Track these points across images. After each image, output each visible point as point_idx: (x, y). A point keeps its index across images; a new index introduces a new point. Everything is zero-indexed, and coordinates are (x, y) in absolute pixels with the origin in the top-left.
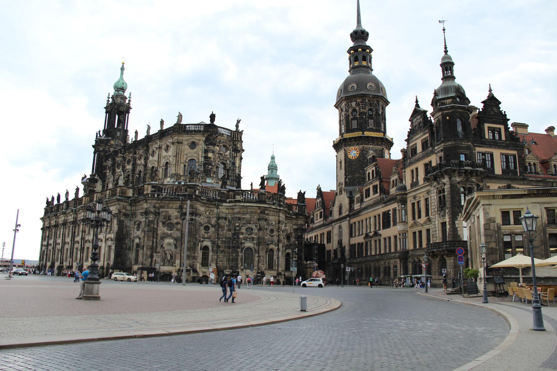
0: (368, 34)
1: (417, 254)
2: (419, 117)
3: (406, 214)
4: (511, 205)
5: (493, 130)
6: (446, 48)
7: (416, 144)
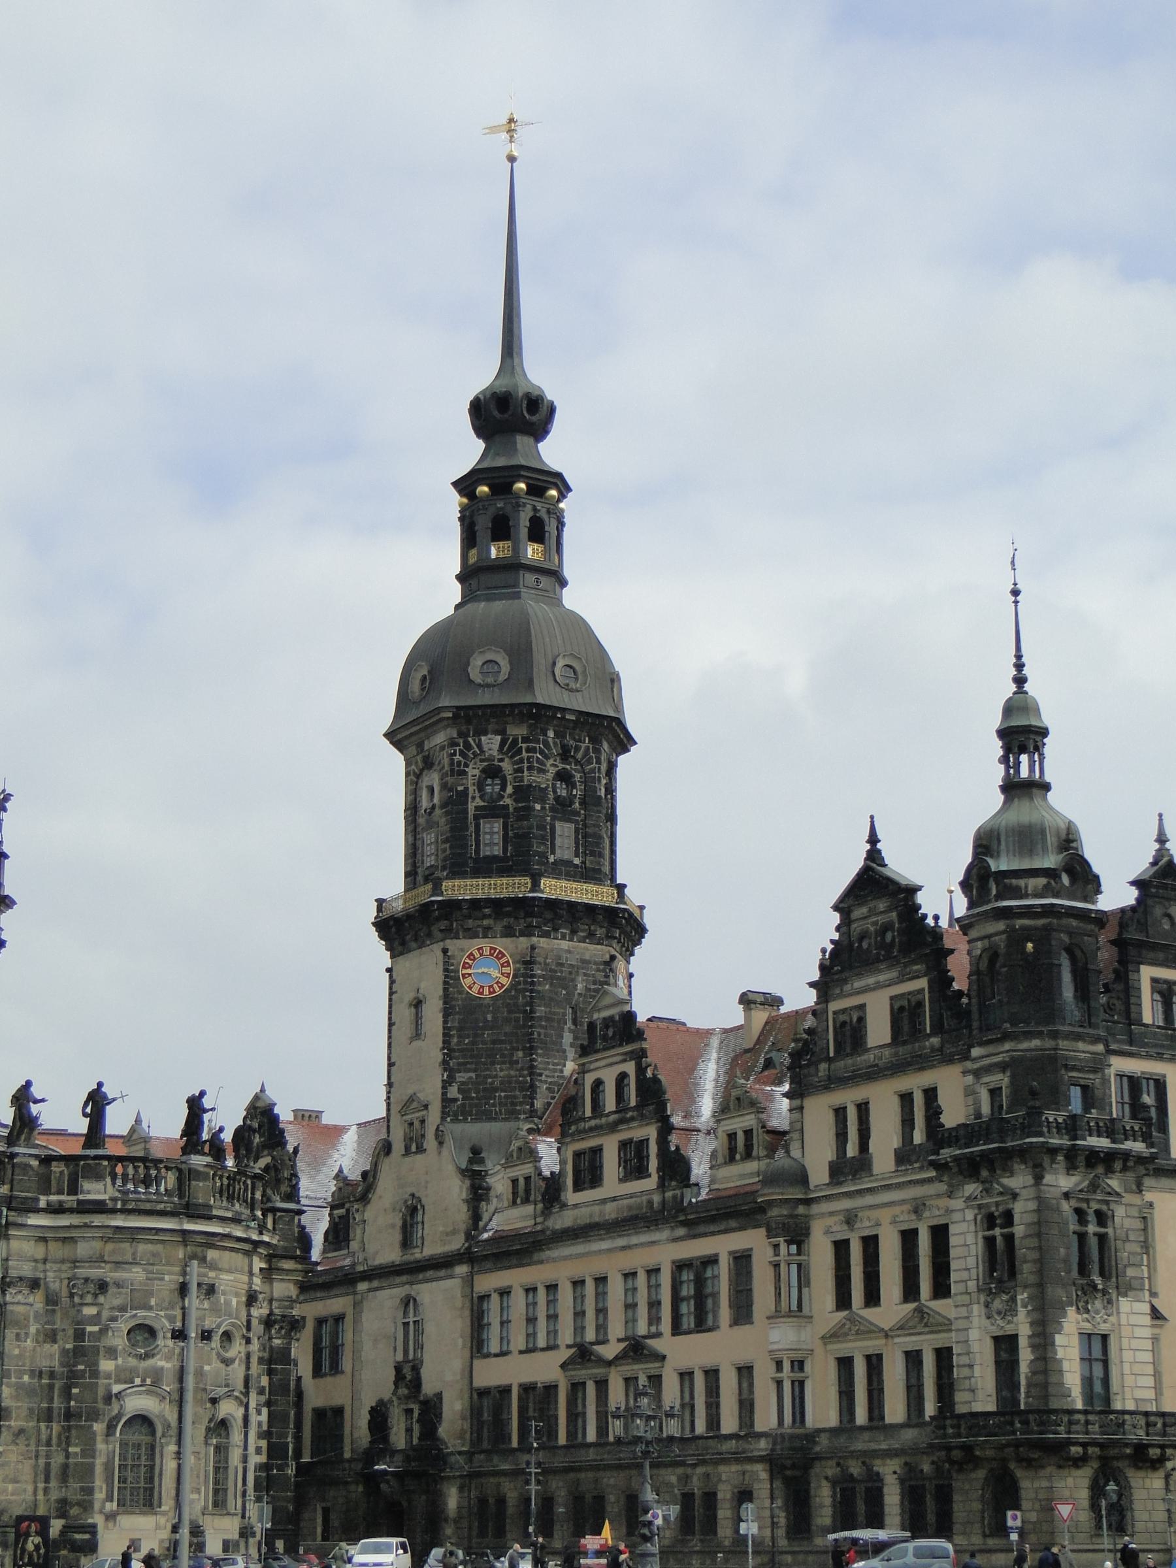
0: (552, 410)
1: (859, 1446)
2: (882, 906)
3: (804, 1279)
6: (1019, 666)
7: (862, 1007)
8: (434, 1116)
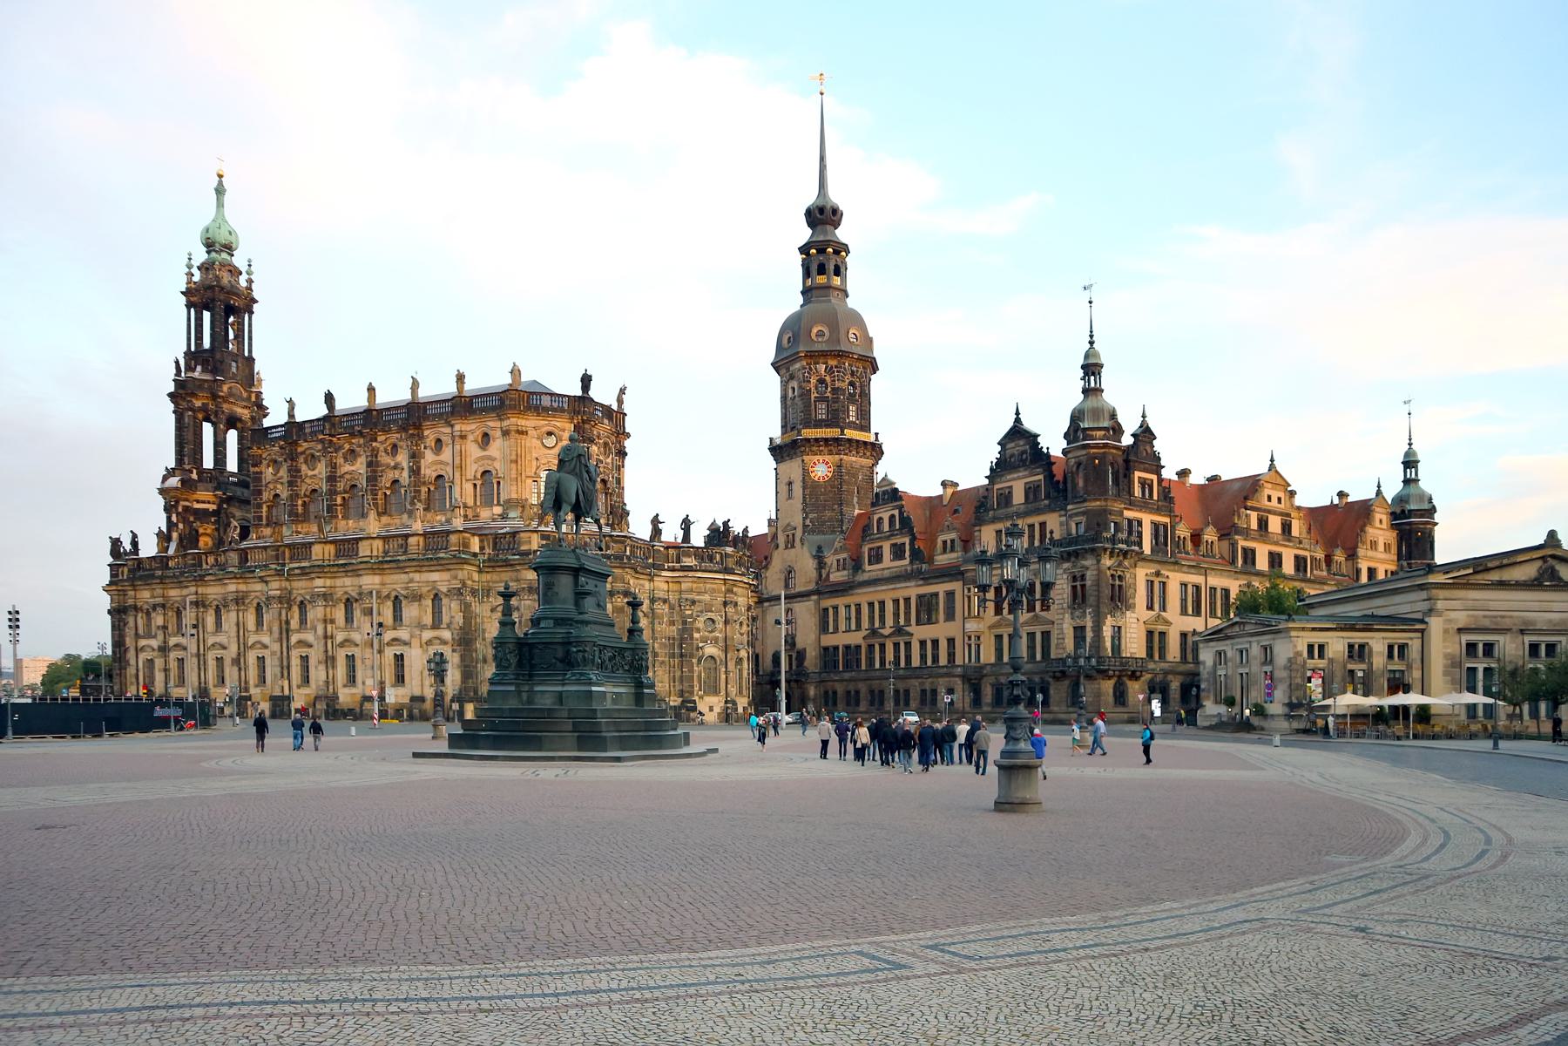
4: (1318, 638)
5: (1143, 482)
8: (799, 534)
